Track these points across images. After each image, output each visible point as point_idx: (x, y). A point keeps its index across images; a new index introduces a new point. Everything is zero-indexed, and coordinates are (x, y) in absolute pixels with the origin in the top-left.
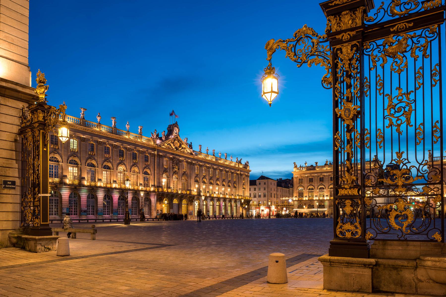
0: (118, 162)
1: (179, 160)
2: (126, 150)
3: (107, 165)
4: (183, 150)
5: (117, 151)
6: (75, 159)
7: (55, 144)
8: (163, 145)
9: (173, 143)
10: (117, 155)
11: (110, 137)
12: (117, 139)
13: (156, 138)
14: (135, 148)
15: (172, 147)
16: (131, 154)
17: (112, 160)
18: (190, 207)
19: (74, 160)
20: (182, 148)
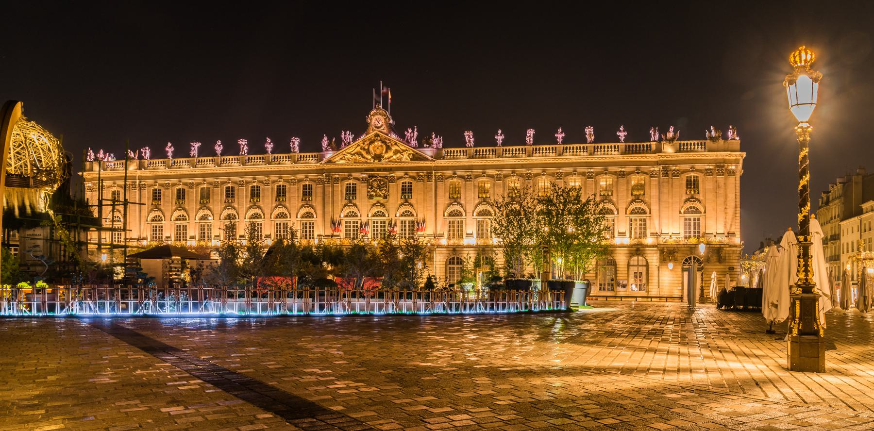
1: (385, 177)
4: (398, 155)
8: (341, 159)
12: (245, 172)
13: (326, 149)
15: (364, 157)
16: (272, 189)
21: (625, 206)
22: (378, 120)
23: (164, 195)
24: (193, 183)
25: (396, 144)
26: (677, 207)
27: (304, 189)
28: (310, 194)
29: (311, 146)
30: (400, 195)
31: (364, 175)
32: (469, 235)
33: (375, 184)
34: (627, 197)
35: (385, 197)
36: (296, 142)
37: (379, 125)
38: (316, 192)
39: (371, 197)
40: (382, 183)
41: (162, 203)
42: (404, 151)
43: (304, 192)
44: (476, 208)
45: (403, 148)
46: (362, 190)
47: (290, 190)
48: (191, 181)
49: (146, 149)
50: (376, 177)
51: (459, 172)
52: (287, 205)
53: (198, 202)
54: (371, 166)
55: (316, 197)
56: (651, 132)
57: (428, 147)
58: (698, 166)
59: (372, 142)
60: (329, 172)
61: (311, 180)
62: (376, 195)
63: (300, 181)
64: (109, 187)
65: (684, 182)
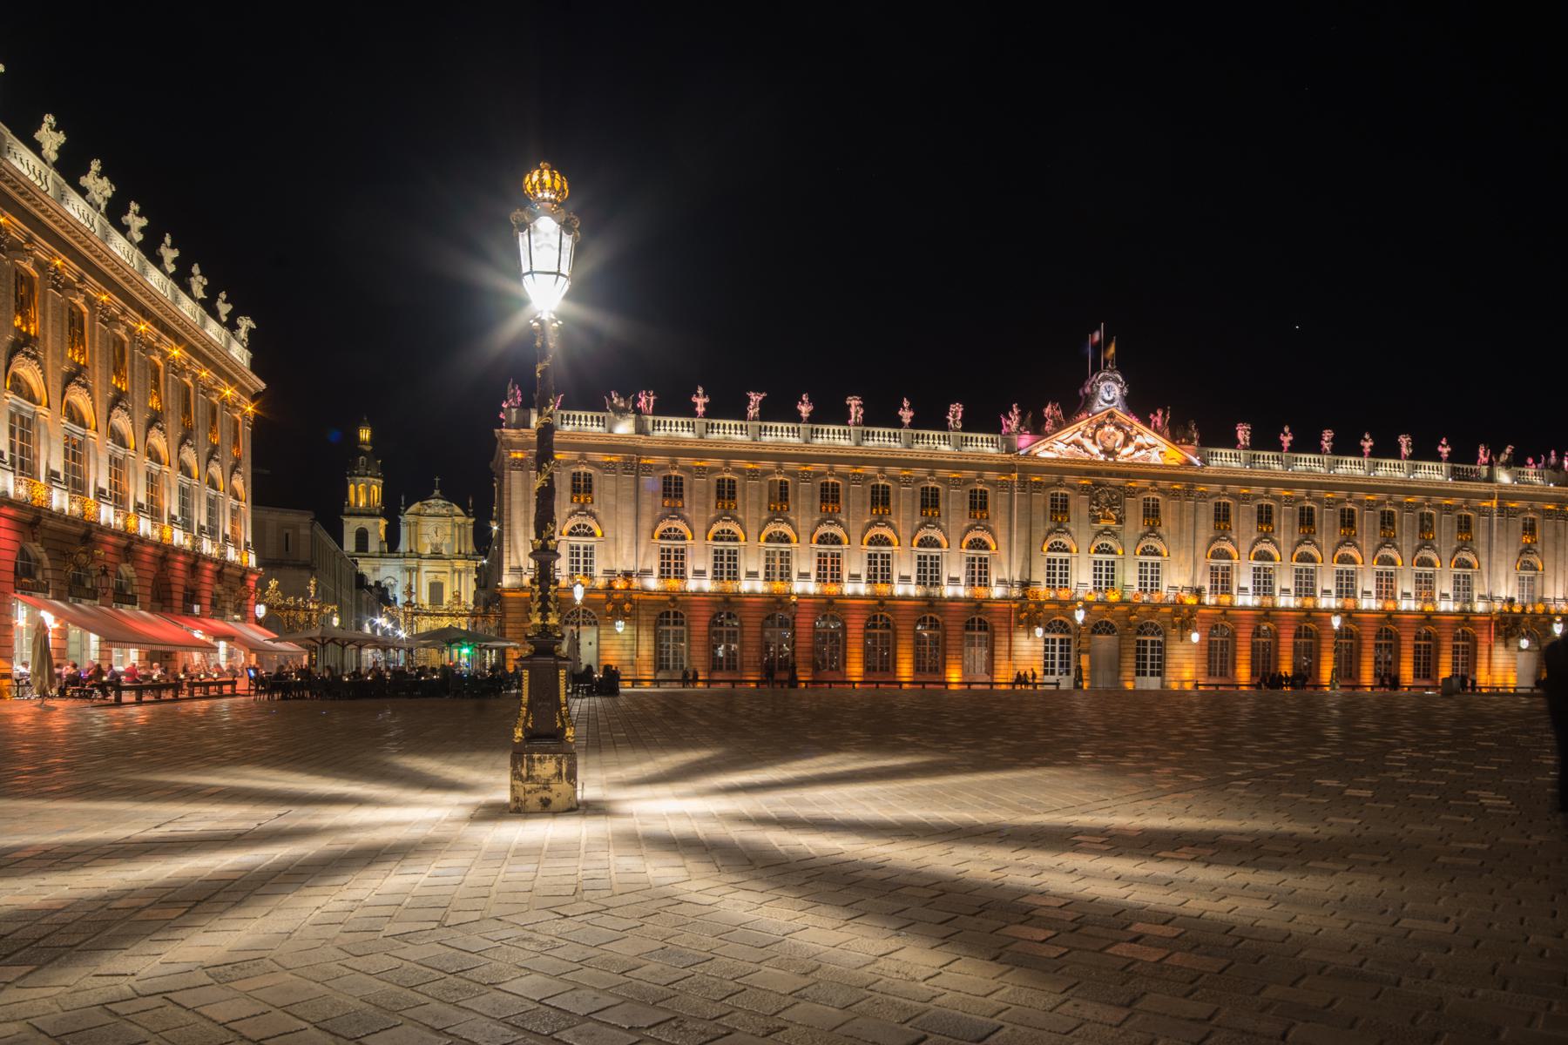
0: (868, 521)
1: (1118, 487)
2: (896, 484)
3: (832, 535)
5: (864, 492)
6: (728, 527)
7: (676, 496)
8: (1047, 449)
9: (1093, 438)
10: (864, 503)
11: (838, 454)
12: (863, 458)
13: (1018, 429)
14: (930, 475)
16: (914, 492)
17: (848, 519)
18: (1177, 647)
19: (729, 531)
20: (1139, 448)
21: (1449, 557)
22: (1109, 392)
23: (691, 489)
24: (756, 470)
25: (1139, 433)
26: (1513, 558)
27: (971, 497)
28: (984, 507)
29: (982, 420)
30: (1141, 518)
31: (1084, 482)
32: (1243, 590)
33: (1102, 499)
34: (1452, 543)
35: (1120, 521)
36: (956, 411)
37: (1109, 398)
38: (995, 504)
39: (1096, 519)
40: (1115, 497)
41: (686, 505)
42: (1154, 446)
43: (971, 503)
44: (1253, 548)
45: (1151, 441)
46: (1080, 506)
47: (947, 497)
48: (751, 466)
49: (648, 395)
50: (1104, 486)
51: (1232, 488)
52: (943, 524)
53: (765, 507)
54: (1098, 467)
55: (995, 512)
56: (1481, 452)
57: (1189, 444)
58: (1538, 505)
59: (1101, 426)
60: (1025, 470)
61: (988, 483)
62: (1104, 518)
63: (967, 482)
64: (569, 463)
65: (1521, 526)
